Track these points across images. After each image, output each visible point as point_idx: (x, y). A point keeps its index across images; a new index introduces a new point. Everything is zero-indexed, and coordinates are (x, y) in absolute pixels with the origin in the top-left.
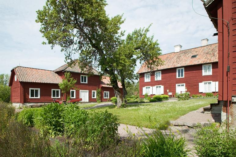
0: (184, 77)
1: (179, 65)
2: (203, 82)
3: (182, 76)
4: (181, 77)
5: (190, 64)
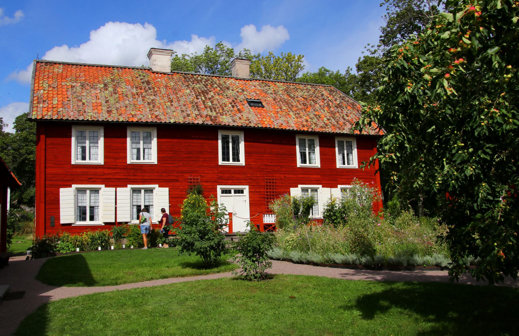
0: (242, 162)
1: (226, 120)
2: (300, 186)
3: (236, 158)
4: (231, 162)
5: (276, 125)
